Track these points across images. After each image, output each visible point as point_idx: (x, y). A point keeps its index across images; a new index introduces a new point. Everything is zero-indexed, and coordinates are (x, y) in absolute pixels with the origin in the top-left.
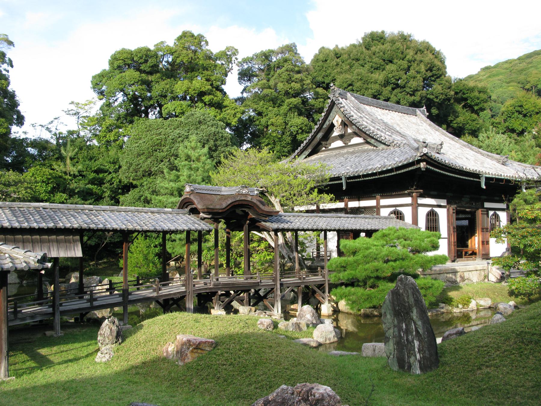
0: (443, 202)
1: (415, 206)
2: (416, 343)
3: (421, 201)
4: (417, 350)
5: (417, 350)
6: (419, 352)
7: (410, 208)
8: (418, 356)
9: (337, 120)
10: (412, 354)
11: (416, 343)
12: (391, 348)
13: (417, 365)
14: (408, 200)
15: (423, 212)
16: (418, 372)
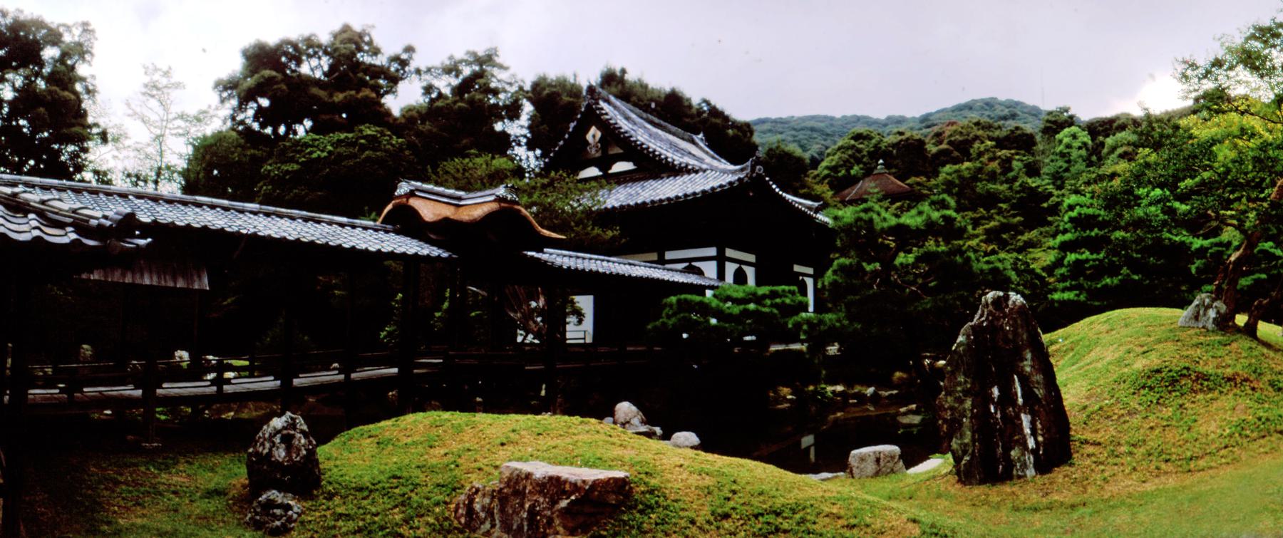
0: (751, 258)
1: (721, 260)
2: (1026, 420)
3: (729, 253)
4: (1027, 431)
5: (1027, 431)
6: (1034, 433)
7: (714, 264)
8: (1031, 443)
9: (593, 134)
10: (1017, 441)
11: (1026, 420)
12: (966, 441)
13: (1030, 459)
14: (712, 251)
15: (730, 268)
16: (1030, 472)
